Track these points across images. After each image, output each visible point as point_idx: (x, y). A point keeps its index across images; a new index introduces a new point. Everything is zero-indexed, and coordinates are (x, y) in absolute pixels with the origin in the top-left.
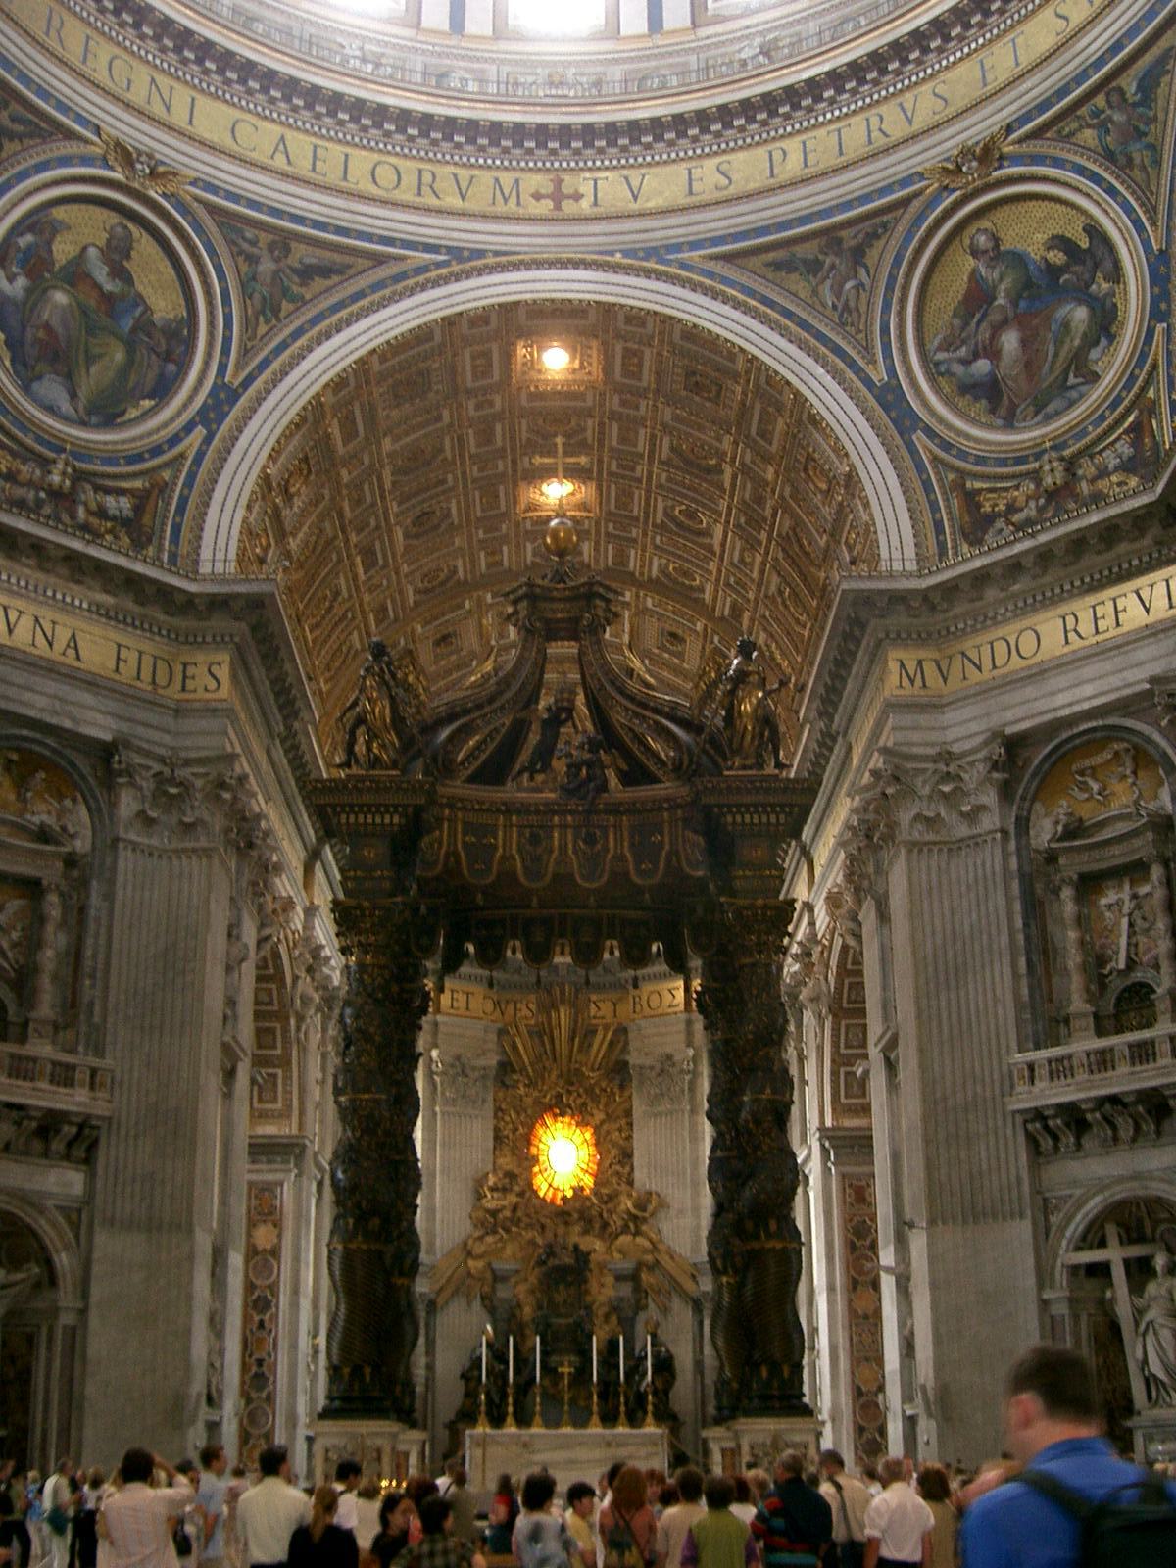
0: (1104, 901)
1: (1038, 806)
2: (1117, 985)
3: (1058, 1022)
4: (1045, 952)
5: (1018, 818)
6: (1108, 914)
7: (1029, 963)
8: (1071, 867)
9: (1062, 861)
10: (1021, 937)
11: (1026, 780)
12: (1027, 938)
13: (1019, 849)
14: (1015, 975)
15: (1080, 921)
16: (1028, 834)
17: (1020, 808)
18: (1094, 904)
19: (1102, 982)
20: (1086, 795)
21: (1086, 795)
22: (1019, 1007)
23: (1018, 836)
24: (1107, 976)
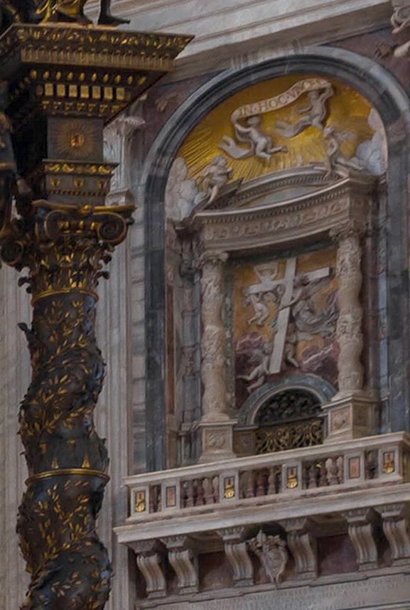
0: (254, 289)
1: (179, 164)
2: (262, 394)
3: (179, 438)
4: (170, 350)
5: (150, 178)
6: (259, 306)
7: (151, 366)
8: (217, 242)
9: (207, 235)
10: (140, 332)
11: (168, 127)
12: (151, 333)
13: (148, 216)
14: (132, 381)
15: (225, 317)
16: (162, 199)
17: (154, 165)
18: (242, 294)
19: (241, 391)
20: (244, 152)
21: (244, 152)
22: (134, 419)
23: (148, 201)
24: (248, 383)
